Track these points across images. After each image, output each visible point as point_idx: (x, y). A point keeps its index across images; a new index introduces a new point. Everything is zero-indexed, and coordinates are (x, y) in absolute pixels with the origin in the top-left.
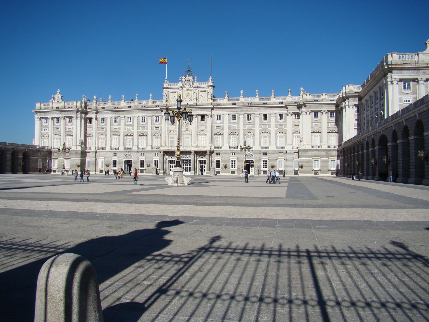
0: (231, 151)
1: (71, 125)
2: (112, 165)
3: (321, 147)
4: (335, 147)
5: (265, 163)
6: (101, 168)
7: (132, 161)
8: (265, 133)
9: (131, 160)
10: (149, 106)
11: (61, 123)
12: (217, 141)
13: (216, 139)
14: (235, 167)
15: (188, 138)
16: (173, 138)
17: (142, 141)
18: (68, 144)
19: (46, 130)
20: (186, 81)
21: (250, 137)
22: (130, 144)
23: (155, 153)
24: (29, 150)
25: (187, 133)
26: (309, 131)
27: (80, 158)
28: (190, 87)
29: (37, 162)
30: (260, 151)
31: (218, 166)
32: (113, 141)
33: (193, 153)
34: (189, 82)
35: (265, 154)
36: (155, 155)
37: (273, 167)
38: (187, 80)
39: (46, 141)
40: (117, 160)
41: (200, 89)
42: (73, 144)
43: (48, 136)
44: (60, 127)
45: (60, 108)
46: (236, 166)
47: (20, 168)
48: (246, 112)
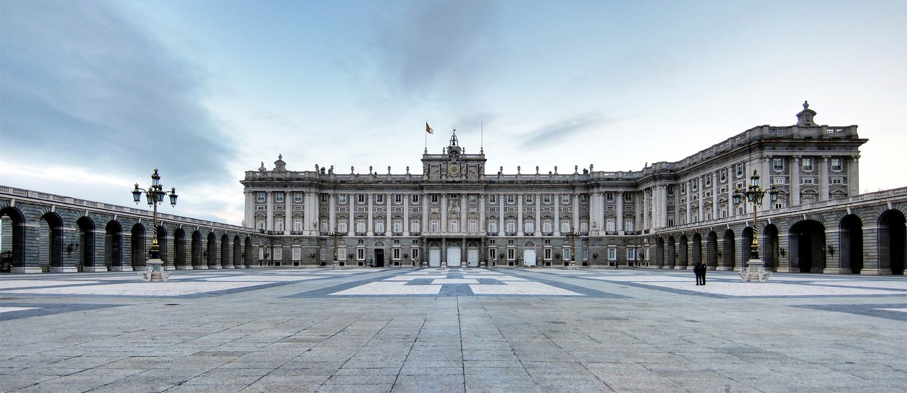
0: (508, 238)
1: (301, 203)
2: (358, 256)
3: (617, 234)
4: (632, 234)
5: (548, 251)
8: (547, 217)
9: (383, 249)
11: (285, 199)
12: (491, 227)
13: (490, 224)
14: (512, 258)
15: (455, 222)
16: (436, 222)
17: (397, 226)
21: (531, 222)
23: (414, 241)
25: (454, 216)
26: (602, 214)
30: (542, 239)
32: (358, 226)
33: (464, 241)
34: (456, 154)
35: (548, 241)
36: (414, 243)
37: (558, 256)
38: (454, 151)
40: (364, 250)
41: (470, 163)
42: (303, 228)
43: (266, 217)
46: (514, 257)
48: (525, 193)
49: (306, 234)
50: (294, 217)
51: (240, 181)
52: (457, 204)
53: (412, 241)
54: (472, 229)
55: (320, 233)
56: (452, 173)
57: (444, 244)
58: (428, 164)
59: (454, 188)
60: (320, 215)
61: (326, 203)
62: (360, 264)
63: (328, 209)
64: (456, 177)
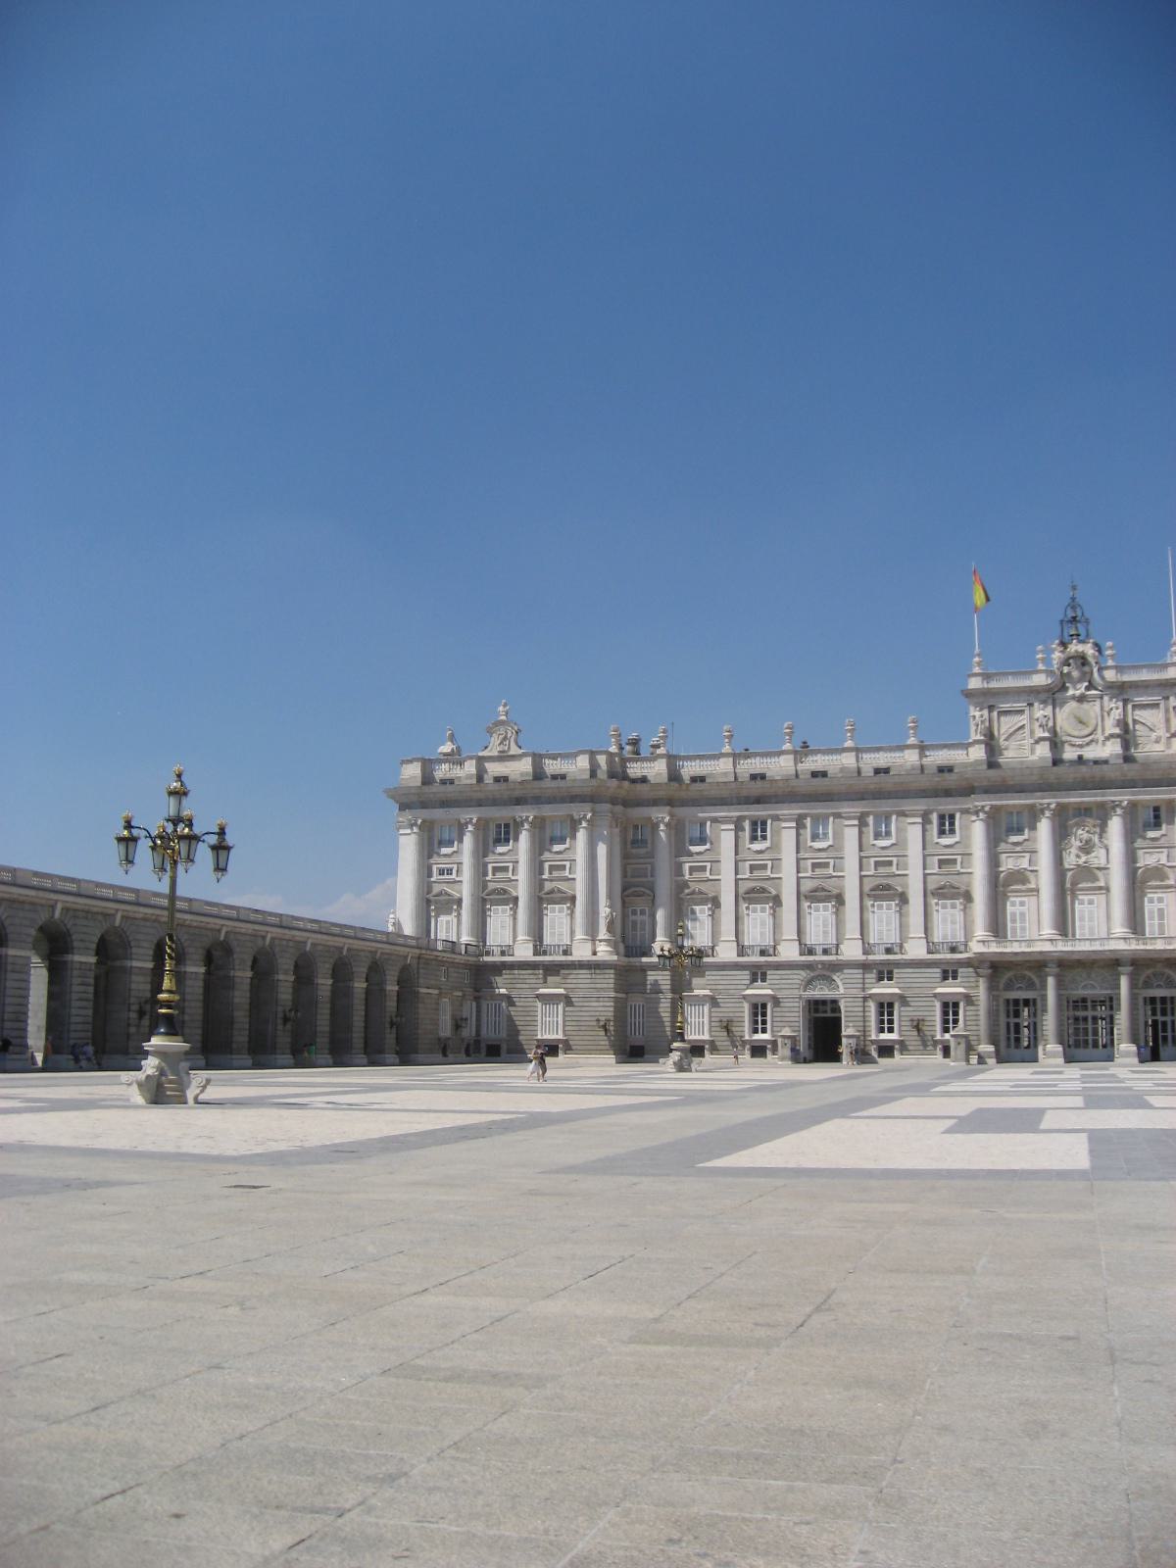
6: (697, 1037)
7: (842, 1005)
9: (835, 1002)
10: (909, 767)
16: (1022, 904)
17: (880, 921)
18: (553, 934)
19: (450, 872)
20: (1070, 658)
22: (825, 932)
24: (415, 961)
27: (613, 994)
28: (1088, 688)
29: (437, 1009)
31: (886, 1026)
34: (1083, 664)
39: (448, 922)
42: (572, 933)
44: (513, 858)
45: (511, 778)
47: (390, 1038)
49: (582, 952)
50: (542, 899)
51: (387, 791)
52: (1096, 839)
53: (937, 972)
54: (1151, 925)
55: (626, 947)
56: (1076, 733)
57: (1051, 981)
58: (986, 705)
59: (1084, 785)
60: (624, 889)
61: (642, 851)
62: (758, 1051)
63: (653, 869)
64: (1088, 744)
